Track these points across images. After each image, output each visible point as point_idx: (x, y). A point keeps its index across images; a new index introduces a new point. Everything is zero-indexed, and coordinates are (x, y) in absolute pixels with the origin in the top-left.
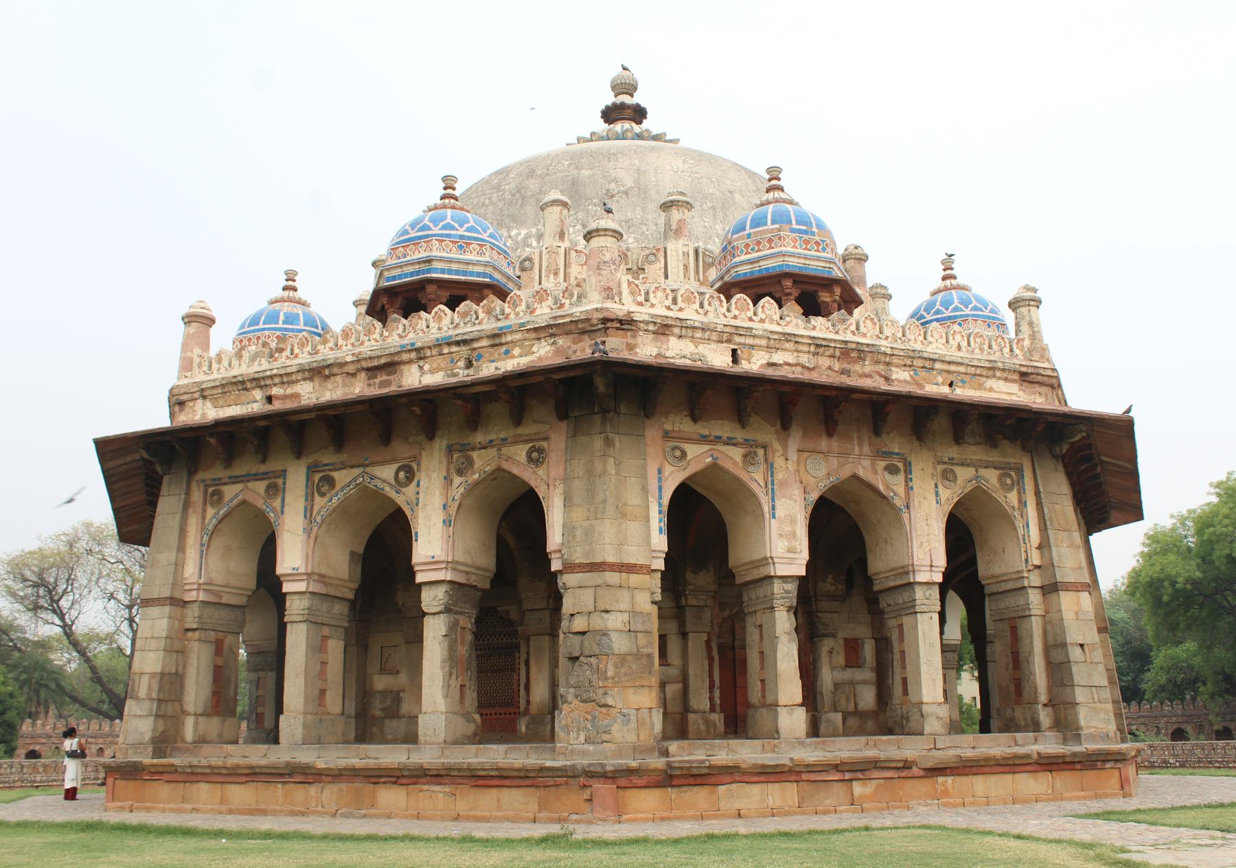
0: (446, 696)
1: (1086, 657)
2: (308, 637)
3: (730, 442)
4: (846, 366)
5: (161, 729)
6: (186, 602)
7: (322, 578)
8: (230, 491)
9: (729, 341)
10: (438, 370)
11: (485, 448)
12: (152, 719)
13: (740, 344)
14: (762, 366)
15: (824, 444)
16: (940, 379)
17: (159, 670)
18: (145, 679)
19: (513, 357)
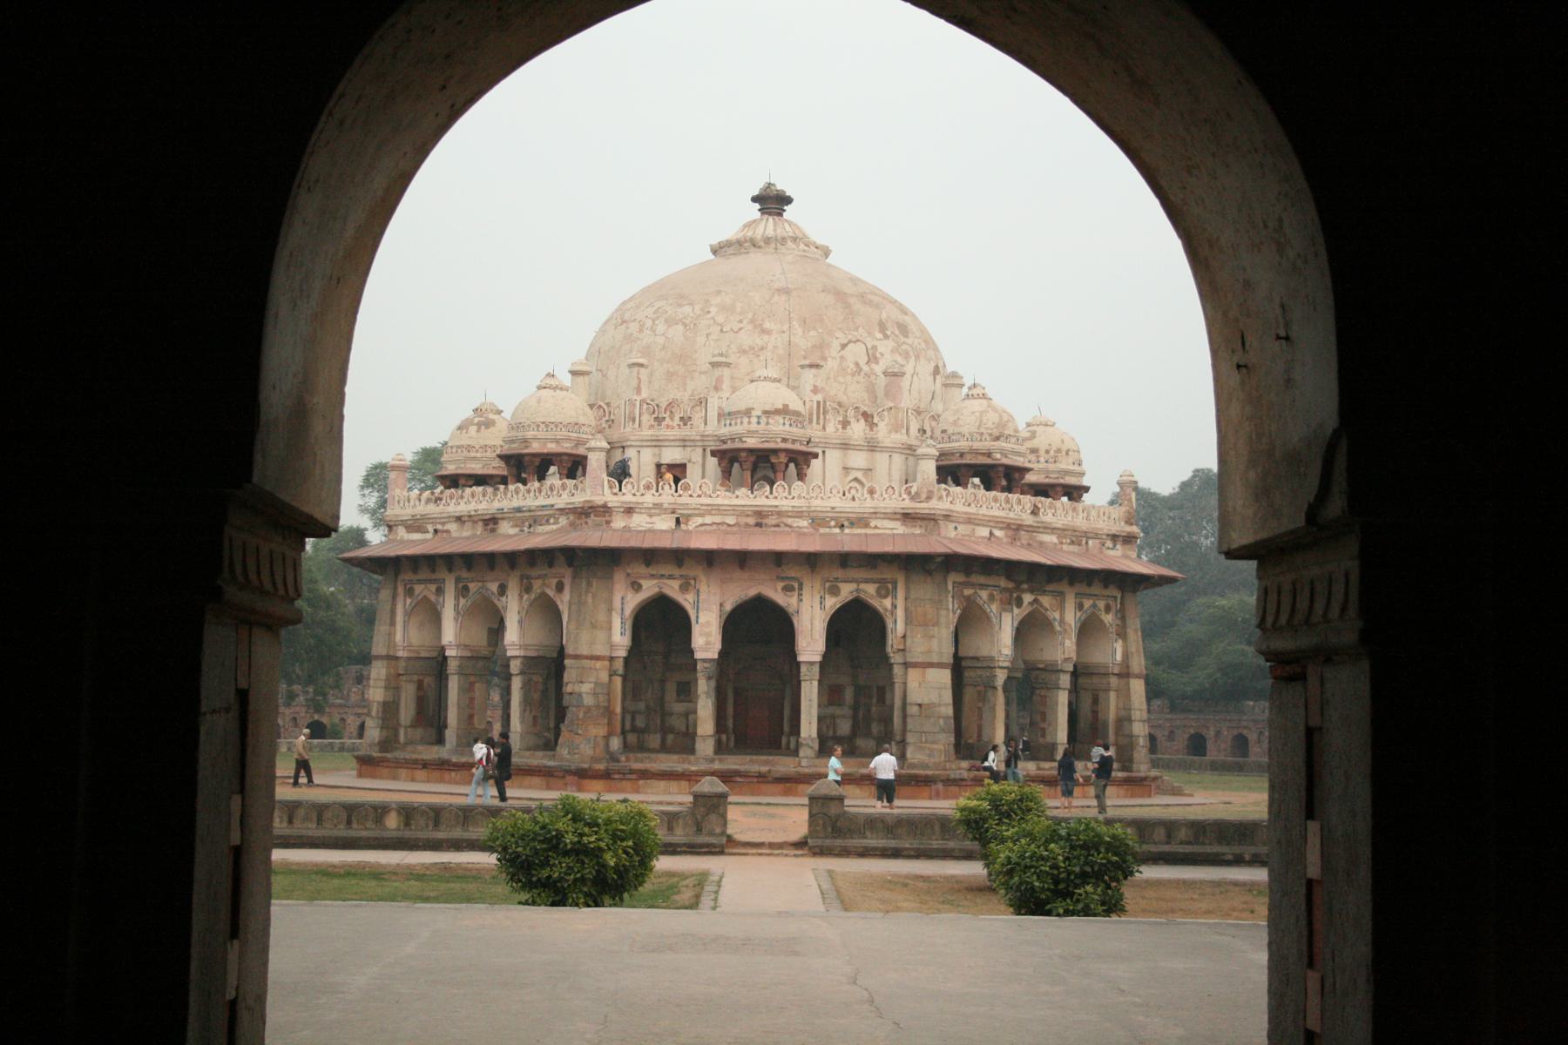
0: (522, 722)
1: (921, 713)
2: (459, 683)
3: (671, 577)
4: (759, 520)
5: (385, 733)
6: (398, 657)
7: (466, 646)
8: (418, 589)
9: (673, 512)
10: (516, 526)
11: (537, 578)
12: (379, 729)
13: (680, 514)
14: (696, 527)
15: (738, 574)
16: (833, 523)
17: (382, 700)
18: (375, 704)
19: (550, 524)
